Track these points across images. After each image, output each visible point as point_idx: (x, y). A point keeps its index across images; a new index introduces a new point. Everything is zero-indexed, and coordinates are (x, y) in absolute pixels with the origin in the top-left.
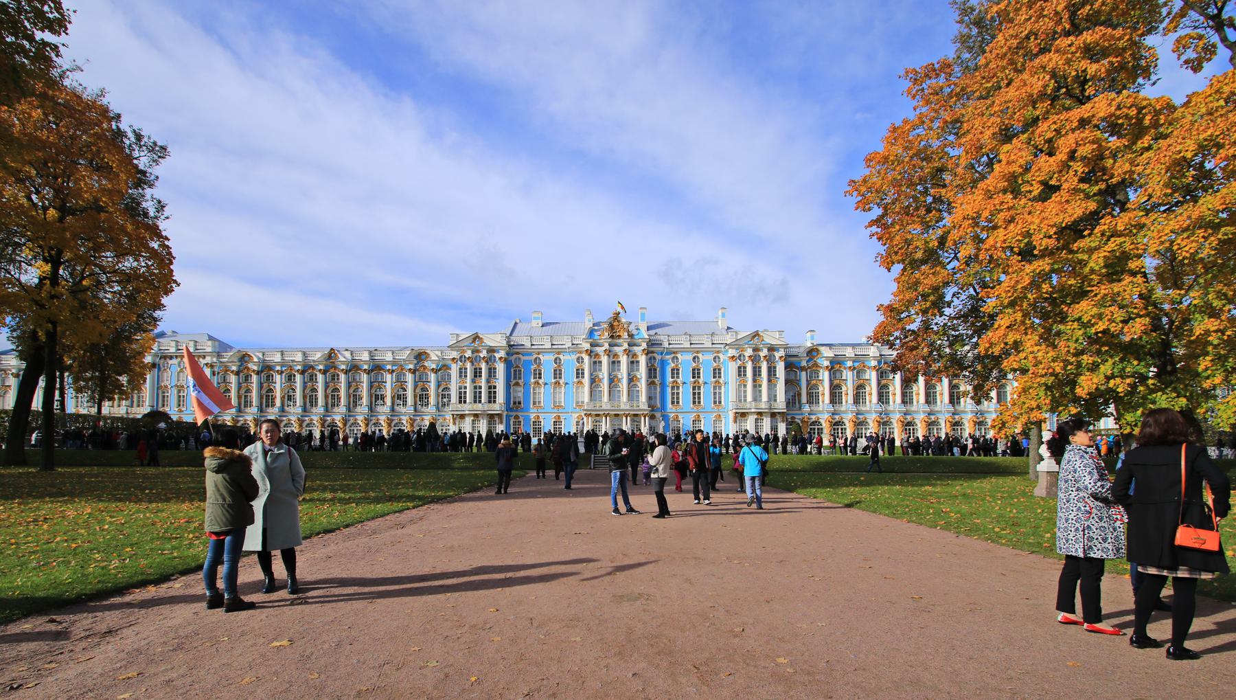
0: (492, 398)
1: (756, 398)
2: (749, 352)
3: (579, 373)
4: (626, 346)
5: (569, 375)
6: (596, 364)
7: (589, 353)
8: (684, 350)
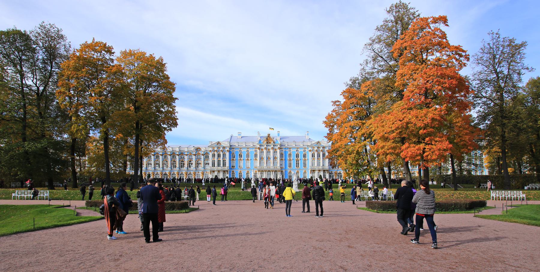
0: (224, 165)
1: (319, 164)
2: (316, 149)
3: (256, 155)
4: (272, 146)
5: (252, 156)
6: (262, 152)
7: (259, 149)
8: (293, 148)
